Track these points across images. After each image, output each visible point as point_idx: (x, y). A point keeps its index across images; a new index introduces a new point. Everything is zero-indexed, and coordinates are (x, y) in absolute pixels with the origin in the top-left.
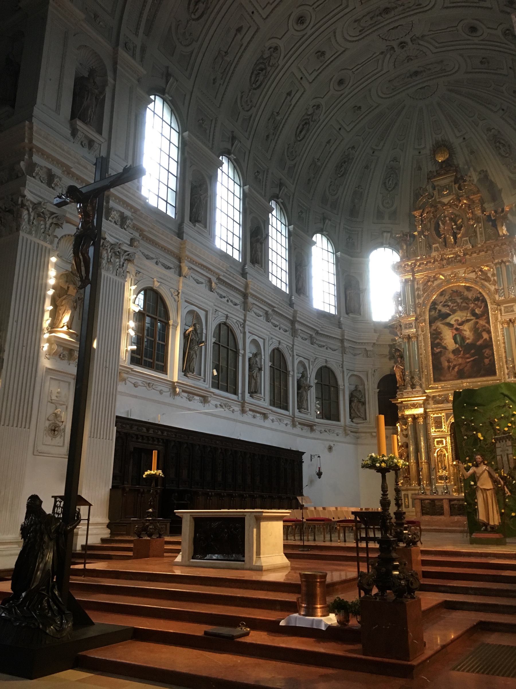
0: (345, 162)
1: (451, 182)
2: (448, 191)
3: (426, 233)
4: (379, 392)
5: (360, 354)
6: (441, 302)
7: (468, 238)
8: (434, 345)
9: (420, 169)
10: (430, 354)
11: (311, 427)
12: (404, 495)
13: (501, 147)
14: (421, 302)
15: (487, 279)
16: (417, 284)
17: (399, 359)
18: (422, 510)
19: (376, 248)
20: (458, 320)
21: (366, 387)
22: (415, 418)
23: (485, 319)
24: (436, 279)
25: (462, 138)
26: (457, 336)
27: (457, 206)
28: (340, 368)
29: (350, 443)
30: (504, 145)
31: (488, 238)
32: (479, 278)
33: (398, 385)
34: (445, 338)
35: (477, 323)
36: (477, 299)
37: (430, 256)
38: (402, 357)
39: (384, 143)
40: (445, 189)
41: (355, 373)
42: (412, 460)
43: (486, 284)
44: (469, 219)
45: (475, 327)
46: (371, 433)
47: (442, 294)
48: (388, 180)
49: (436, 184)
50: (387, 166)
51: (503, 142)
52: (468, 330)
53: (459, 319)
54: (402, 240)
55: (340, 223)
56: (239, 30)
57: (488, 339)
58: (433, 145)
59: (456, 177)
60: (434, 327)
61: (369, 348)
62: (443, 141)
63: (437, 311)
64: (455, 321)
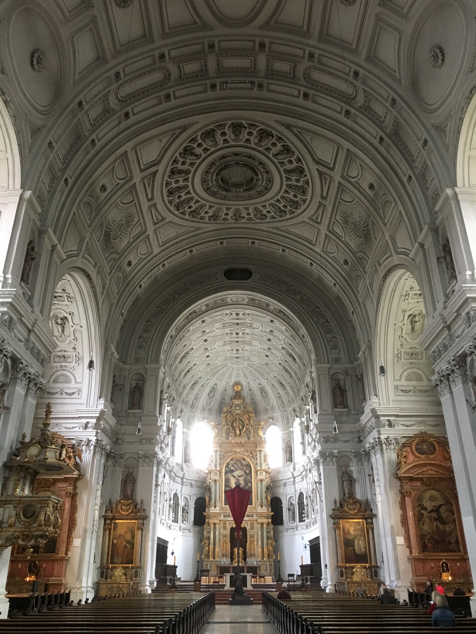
0: (195, 384)
3: (228, 427)
9: (225, 390)
10: (224, 490)
11: (169, 527)
15: (253, 457)
24: (230, 452)
27: (243, 417)
30: (265, 393)
31: (254, 437)
33: (206, 505)
35: (246, 477)
36: (247, 465)
37: (228, 439)
38: (210, 489)
41: (185, 496)
42: (211, 547)
44: (247, 425)
47: (232, 460)
56: (185, 346)
59: (244, 402)
60: (227, 476)
61: (193, 482)
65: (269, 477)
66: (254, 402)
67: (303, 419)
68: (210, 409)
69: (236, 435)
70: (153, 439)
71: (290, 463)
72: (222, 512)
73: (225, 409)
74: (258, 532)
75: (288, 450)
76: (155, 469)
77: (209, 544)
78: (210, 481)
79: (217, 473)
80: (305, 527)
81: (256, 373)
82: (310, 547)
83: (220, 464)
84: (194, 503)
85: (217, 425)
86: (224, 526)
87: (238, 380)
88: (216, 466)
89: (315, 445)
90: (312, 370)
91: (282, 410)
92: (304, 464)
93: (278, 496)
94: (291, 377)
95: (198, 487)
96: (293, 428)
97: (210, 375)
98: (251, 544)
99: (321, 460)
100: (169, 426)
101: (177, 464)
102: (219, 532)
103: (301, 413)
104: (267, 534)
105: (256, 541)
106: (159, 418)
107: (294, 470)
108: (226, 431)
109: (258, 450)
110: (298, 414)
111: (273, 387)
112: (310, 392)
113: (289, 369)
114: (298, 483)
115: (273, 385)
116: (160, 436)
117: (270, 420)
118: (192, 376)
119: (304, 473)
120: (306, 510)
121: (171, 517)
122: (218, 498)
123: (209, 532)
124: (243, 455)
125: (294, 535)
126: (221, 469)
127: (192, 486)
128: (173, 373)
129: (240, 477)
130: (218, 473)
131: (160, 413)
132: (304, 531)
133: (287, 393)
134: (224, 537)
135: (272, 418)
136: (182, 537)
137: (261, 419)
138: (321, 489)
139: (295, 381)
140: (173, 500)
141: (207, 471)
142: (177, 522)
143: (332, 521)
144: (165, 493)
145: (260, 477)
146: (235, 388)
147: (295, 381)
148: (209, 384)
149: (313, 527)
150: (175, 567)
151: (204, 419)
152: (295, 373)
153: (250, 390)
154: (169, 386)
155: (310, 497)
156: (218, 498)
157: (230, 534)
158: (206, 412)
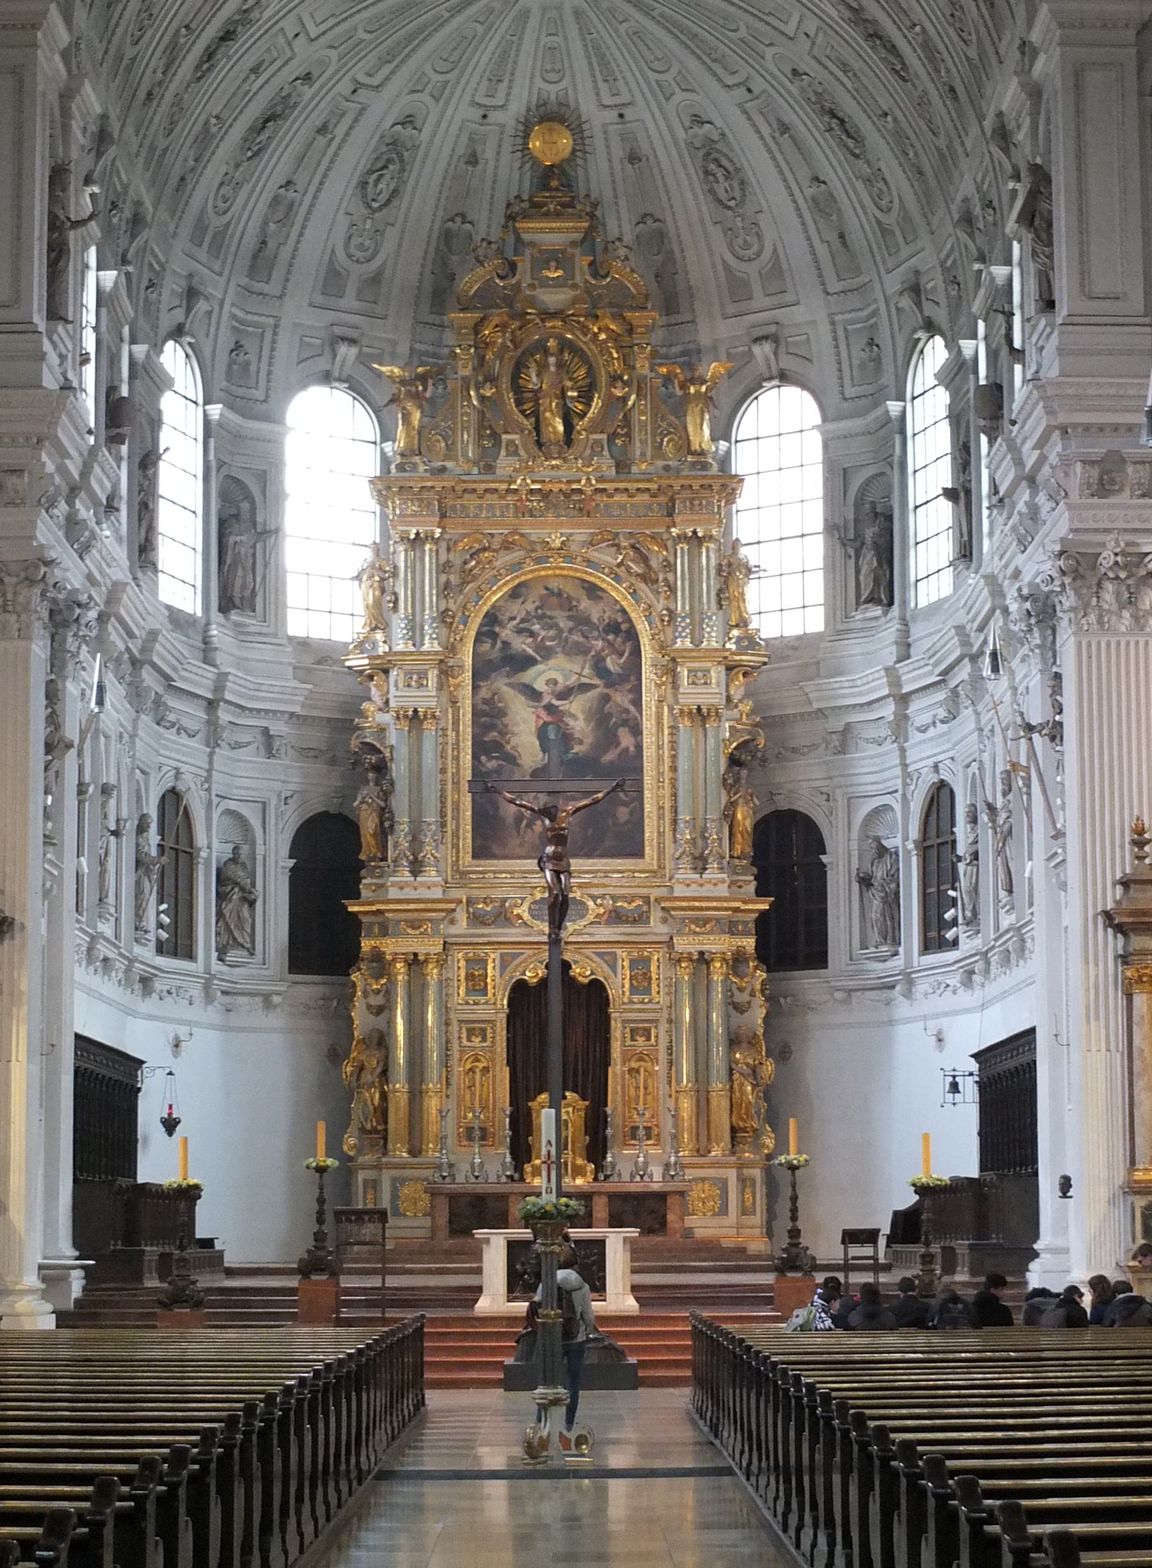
1: (573, 244)
2: (560, 273)
4: (292, 870)
5: (249, 743)
6: (513, 619)
7: (604, 436)
8: (480, 748)
9: (473, 160)
10: (467, 774)
11: (146, 982)
12: (365, 1181)
13: (719, 175)
14: (453, 607)
15: (647, 578)
16: (449, 549)
17: (371, 775)
18: (450, 1222)
19: (303, 385)
20: (555, 682)
21: (260, 850)
22: (415, 962)
23: (630, 691)
24: (507, 546)
25: (615, 113)
26: (551, 727)
27: (585, 330)
28: (202, 793)
29: (213, 1027)
30: (728, 175)
32: (628, 569)
33: (362, 857)
34: (516, 729)
35: (606, 698)
36: (613, 628)
37: (489, 468)
38: (381, 768)
39: (393, 72)
40: (553, 264)
41: (233, 805)
43: (643, 586)
44: (615, 379)
45: (600, 709)
46: (267, 998)
47: (515, 594)
48: (375, 175)
49: (526, 237)
50: (382, 137)
51: (725, 162)
52: (581, 717)
53: (560, 679)
54: (409, 393)
55: (222, 303)
57: (632, 749)
58: (529, 110)
59: (589, 233)
60: (484, 693)
61: (278, 728)
62: (560, 104)
63: (499, 645)
64: (548, 683)
65: (746, 696)
66: (661, 236)
67: (967, 346)
68: (376, 279)
69: (539, 444)
70: (17, 472)
71: (877, 611)
72: (462, 894)
73: (470, 282)
74: (675, 1006)
75: (869, 533)
76: (39, 649)
77: (385, 1074)
78: (386, 718)
79: (423, 675)
80: (954, 980)
81: (668, 40)
82: (982, 1086)
83: (444, 617)
84: (285, 850)
85: (423, 378)
86: (470, 977)
87: (552, 92)
88: (414, 630)
89: (1034, 511)
90: (1035, 37)
91: (835, 286)
92: (961, 618)
93: (801, 806)
94: (901, 72)
95: (306, 753)
96: (901, 397)
97: (372, 59)
98: (634, 1072)
99: (1069, 600)
100: (112, 389)
101: (177, 619)
102: (444, 1010)
103: (957, 306)
104: (727, 1018)
105: (663, 1056)
106: (47, 346)
107: (904, 656)
108: (482, 414)
109: (683, 537)
110: (940, 315)
111: (785, 139)
112: (1017, 177)
113: (889, 27)
114: (923, 730)
115: (784, 128)
116: (65, 454)
117: (762, 351)
118: (255, 70)
119: (964, 672)
120: (964, 882)
121: (150, 921)
122: (431, 818)
123: (379, 1010)
124: (589, 562)
125: (891, 1023)
126: (451, 649)
127: (270, 752)
128: (130, 52)
129: (565, 694)
130: (433, 675)
131: (56, 312)
132: (948, 1001)
133: (874, 179)
134: (471, 1033)
135: (774, 338)
136: (214, 1036)
137: (705, 340)
138: (1060, 766)
139: (922, 103)
140: (162, 832)
141: (358, 661)
142: (190, 956)
143: (1115, 943)
144: (106, 790)
145: (691, 696)
146: (535, 144)
147: (922, 103)
148: (370, 120)
149: (1002, 981)
150: (189, 1194)
151: (336, 340)
152: (928, 49)
153: (634, 158)
154: (102, 139)
155: (991, 808)
156: (431, 818)
157: (510, 1019)
158: (350, 300)
